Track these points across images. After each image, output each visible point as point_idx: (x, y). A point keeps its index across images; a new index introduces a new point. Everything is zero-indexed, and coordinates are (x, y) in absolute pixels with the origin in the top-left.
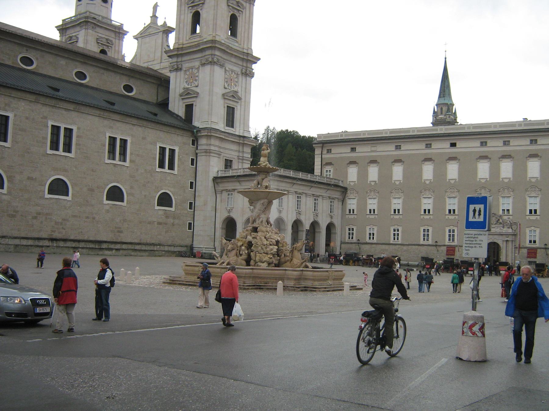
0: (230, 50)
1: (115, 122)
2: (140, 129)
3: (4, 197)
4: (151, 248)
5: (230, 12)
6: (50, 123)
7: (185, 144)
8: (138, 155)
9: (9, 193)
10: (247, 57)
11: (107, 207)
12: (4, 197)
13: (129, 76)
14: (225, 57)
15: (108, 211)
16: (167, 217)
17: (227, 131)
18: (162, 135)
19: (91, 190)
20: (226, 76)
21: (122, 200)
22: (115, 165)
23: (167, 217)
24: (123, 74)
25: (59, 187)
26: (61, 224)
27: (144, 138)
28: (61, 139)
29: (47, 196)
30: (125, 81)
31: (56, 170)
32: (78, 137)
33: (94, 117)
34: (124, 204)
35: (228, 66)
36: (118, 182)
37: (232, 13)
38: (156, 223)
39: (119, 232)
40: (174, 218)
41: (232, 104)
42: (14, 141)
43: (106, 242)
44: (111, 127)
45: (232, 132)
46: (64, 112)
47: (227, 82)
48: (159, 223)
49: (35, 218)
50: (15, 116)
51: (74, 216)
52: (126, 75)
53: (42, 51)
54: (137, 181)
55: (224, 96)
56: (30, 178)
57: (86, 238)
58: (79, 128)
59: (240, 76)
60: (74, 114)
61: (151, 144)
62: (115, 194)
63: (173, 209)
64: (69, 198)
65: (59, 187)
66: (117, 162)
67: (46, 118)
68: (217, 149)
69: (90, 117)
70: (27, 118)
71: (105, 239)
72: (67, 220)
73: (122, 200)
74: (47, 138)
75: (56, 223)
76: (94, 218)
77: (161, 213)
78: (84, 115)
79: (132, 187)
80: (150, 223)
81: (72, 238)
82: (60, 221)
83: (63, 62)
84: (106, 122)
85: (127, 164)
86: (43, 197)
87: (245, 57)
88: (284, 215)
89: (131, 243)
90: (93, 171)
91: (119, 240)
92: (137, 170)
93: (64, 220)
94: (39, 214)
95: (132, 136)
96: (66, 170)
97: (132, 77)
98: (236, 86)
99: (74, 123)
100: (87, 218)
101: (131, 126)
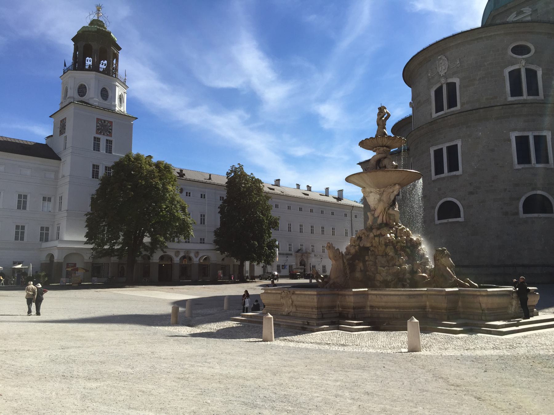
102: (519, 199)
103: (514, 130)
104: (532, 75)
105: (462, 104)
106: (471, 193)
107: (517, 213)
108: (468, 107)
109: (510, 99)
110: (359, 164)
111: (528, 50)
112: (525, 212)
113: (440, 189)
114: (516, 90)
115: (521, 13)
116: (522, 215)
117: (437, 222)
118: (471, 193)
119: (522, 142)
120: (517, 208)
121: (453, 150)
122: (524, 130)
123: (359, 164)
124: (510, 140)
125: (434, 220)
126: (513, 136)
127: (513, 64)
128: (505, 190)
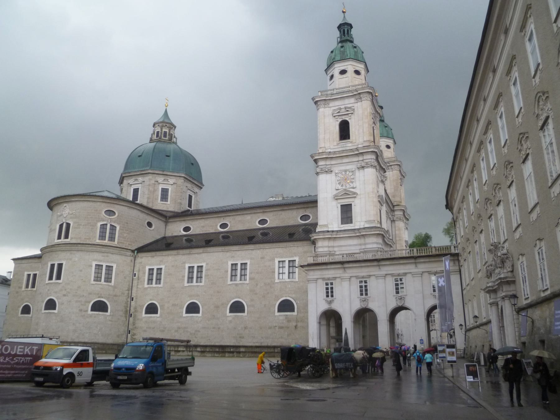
0: (334, 154)
1: (236, 252)
2: (258, 251)
3: (158, 319)
4: (272, 350)
5: (337, 121)
6: (187, 266)
7: (305, 252)
8: (257, 273)
9: (161, 316)
10: (358, 150)
11: (230, 319)
12: (158, 319)
13: (304, 208)
14: (328, 162)
15: (230, 322)
16: (289, 321)
17: (343, 229)
18: (280, 250)
19: (217, 307)
20: (338, 178)
21: (243, 311)
22: (236, 285)
23: (289, 321)
24: (298, 208)
25: (193, 308)
26: (194, 334)
27: (262, 258)
28: (196, 273)
29: (185, 315)
30: (302, 212)
31: (191, 296)
32: (207, 270)
33: (219, 253)
34: (246, 314)
35: (336, 169)
36: (239, 298)
37: (340, 120)
38: (277, 328)
39: (240, 337)
40: (297, 321)
41: (346, 202)
42: (164, 283)
43: (228, 346)
44: (233, 257)
45: (353, 228)
46: (197, 255)
47: (339, 183)
48: (281, 328)
49: (176, 331)
50: (166, 267)
51: (204, 328)
52: (301, 208)
53: (233, 215)
54: (256, 294)
55: (336, 197)
56: (174, 305)
57: (213, 344)
58: (207, 264)
59: (357, 171)
60: (204, 255)
61: (270, 261)
62: (237, 307)
63: (295, 313)
64: (200, 315)
65: (193, 308)
66: (238, 281)
67: (184, 263)
68: (326, 249)
69: (216, 254)
70: (173, 266)
71: (228, 344)
72: (199, 331)
73: (243, 311)
74: (184, 276)
75: (191, 334)
76: (219, 328)
77: (281, 318)
78: (211, 254)
79: (252, 300)
80: (270, 328)
81: (202, 344)
82: (194, 332)
83: (248, 217)
84: (228, 254)
85: (247, 282)
86: (182, 317)
87: (357, 153)
88: (336, 306)
89: (251, 347)
90: (218, 292)
91: (241, 344)
92: (257, 285)
93: (196, 331)
94: (179, 328)
95: (251, 259)
96: (198, 296)
97: (307, 208)
98: (352, 182)
99: (204, 262)
100: (214, 328)
101: (250, 252)
102: (90, 302)
103: (95, 260)
104: (113, 228)
105: (72, 239)
106: (64, 295)
107: (87, 311)
108: (74, 241)
109: (98, 241)
110: (14, 260)
111: (114, 213)
112: (92, 310)
113: (48, 290)
114: (102, 237)
115: (136, 180)
116: (90, 312)
117: (43, 311)
118: (64, 295)
119: (99, 267)
120: (88, 307)
121: (60, 266)
122: (100, 261)
123: (14, 260)
124: (92, 266)
125: (41, 310)
126: (94, 264)
127: (103, 221)
128: (83, 296)
